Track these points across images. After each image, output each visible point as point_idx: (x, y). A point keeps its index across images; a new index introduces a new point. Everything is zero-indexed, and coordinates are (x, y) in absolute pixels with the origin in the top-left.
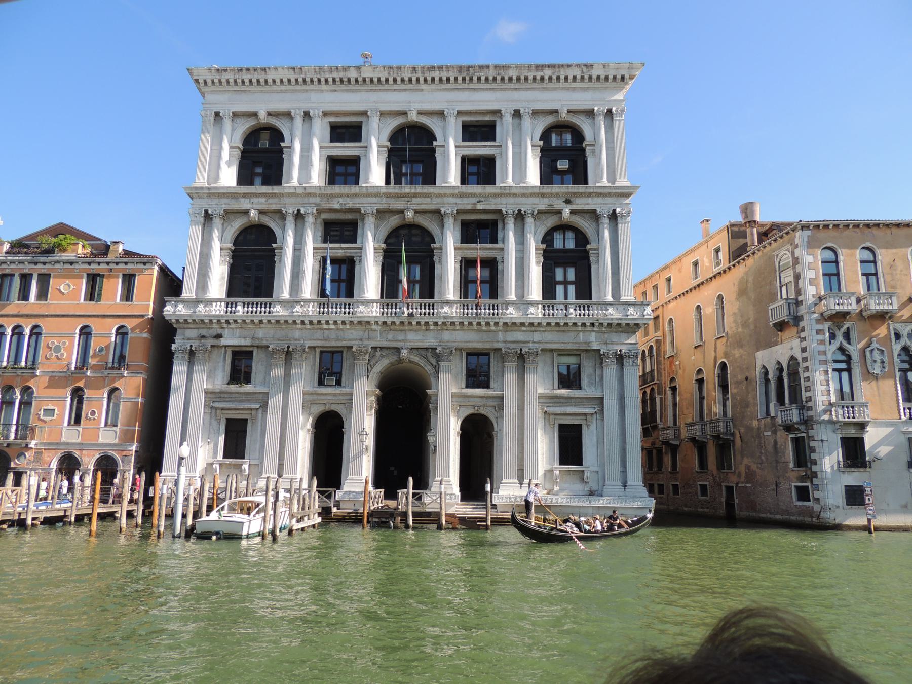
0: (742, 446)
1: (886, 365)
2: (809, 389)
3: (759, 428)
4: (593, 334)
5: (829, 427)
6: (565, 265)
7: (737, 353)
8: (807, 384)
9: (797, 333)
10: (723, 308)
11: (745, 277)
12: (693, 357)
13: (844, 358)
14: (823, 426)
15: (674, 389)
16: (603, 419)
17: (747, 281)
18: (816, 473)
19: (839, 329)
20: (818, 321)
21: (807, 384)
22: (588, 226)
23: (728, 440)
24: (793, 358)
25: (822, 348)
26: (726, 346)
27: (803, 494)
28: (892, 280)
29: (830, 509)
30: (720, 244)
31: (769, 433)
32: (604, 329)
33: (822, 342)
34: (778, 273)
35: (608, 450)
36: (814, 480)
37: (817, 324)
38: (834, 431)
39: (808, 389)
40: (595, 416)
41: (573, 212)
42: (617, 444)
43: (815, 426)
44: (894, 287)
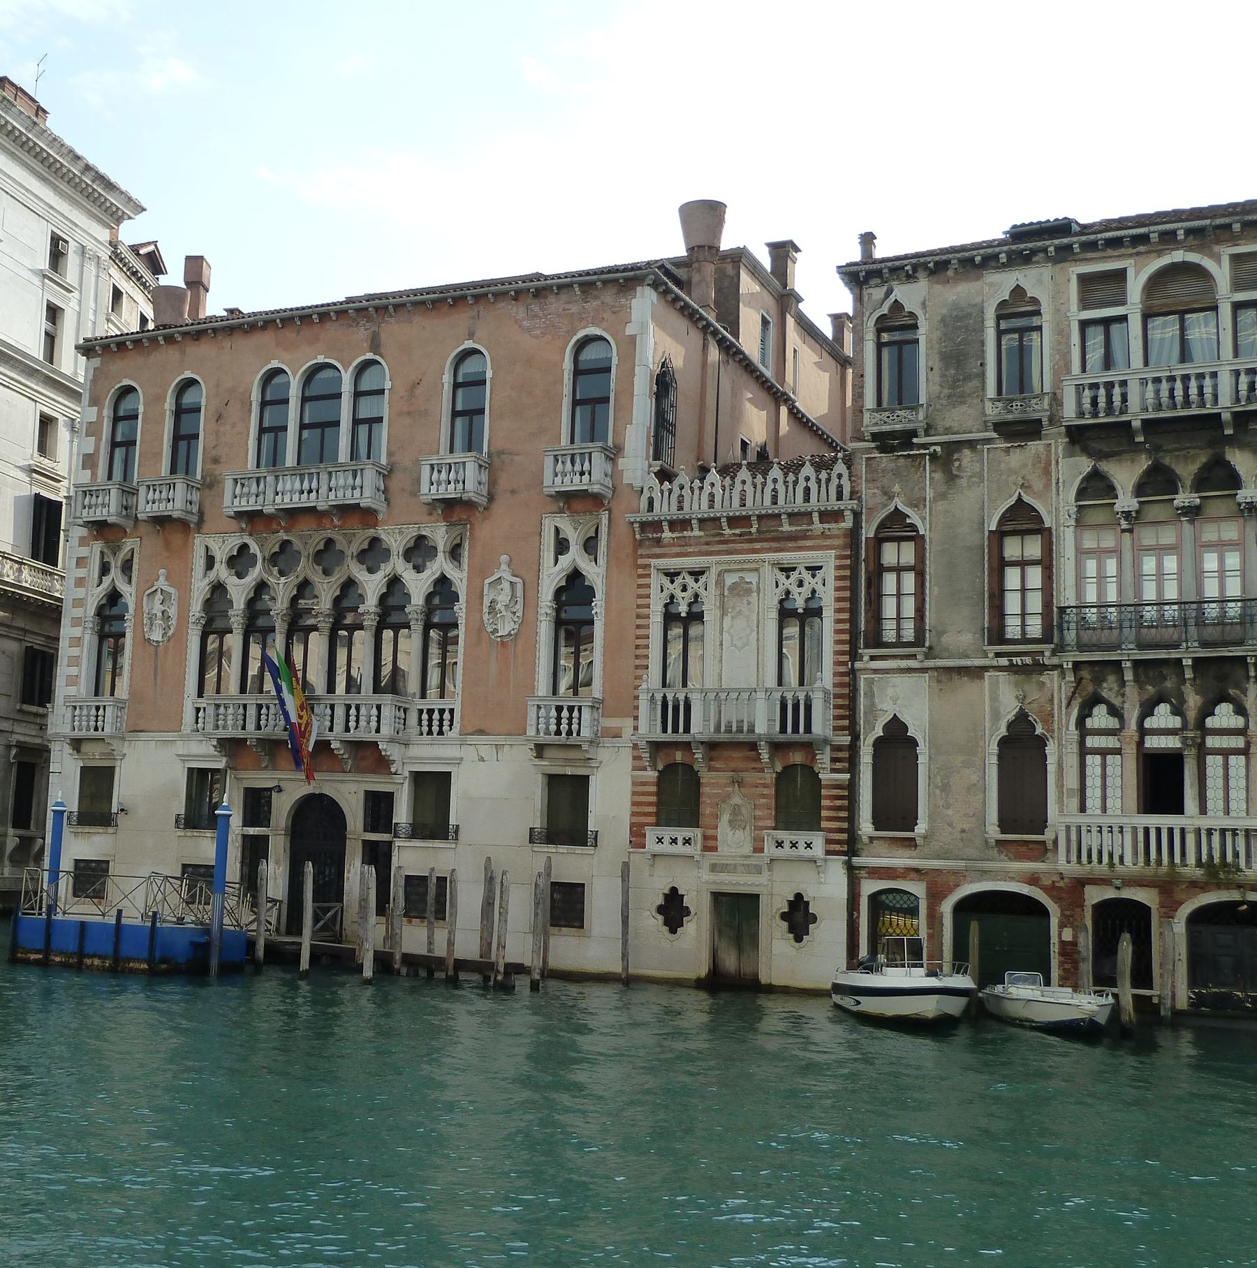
1: (173, 622)
20: (83, 542)
25: (80, 593)
33: (80, 582)
44: (216, 461)
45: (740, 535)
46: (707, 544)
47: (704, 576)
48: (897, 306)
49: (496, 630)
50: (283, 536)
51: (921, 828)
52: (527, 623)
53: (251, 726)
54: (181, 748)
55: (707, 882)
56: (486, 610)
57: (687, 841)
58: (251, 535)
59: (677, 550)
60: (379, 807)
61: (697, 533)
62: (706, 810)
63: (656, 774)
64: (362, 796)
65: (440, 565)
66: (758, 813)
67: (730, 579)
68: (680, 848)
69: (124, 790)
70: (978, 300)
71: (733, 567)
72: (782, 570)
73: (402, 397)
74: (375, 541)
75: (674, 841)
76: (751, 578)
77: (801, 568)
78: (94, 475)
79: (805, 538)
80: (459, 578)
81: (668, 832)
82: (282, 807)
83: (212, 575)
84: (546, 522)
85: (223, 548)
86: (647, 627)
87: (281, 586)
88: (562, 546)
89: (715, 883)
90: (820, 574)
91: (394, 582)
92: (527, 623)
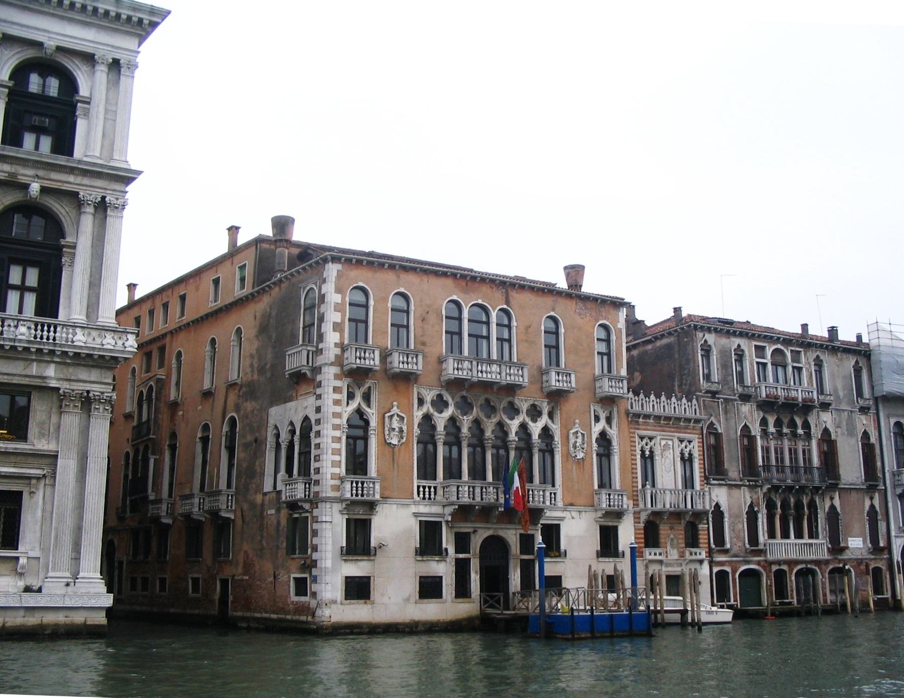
0: (243, 528)
1: (405, 434)
2: (318, 458)
3: (263, 505)
4: (52, 367)
5: (337, 507)
6: (25, 264)
7: (249, 406)
9: (314, 388)
10: (241, 344)
11: (268, 310)
12: (200, 407)
13: (362, 423)
14: (328, 505)
15: (173, 448)
16: (54, 485)
17: (270, 315)
18: (316, 561)
19: (359, 388)
20: (337, 377)
21: (318, 452)
22: (64, 213)
23: (228, 519)
24: (306, 419)
25: (338, 409)
26: (239, 396)
27: (302, 587)
28: (422, 336)
29: (326, 604)
30: (247, 262)
31: (273, 511)
32: (68, 361)
33: (337, 402)
35: (57, 529)
36: (313, 570)
37: (335, 379)
38: (340, 511)
39: (317, 459)
40: (42, 482)
41: (44, 190)
42: (69, 522)
43: (320, 505)
44: (424, 344)
45: (667, 424)
46: (655, 426)
47: (655, 439)
48: (706, 341)
49: (576, 456)
50: (464, 393)
51: (728, 546)
52: (588, 454)
53: (478, 499)
54: (414, 509)
55: (666, 571)
56: (571, 445)
57: (660, 554)
58: (447, 390)
59: (644, 427)
60: (527, 542)
61: (651, 421)
62: (662, 541)
63: (644, 525)
64: (518, 536)
65: (544, 420)
66: (680, 541)
67: (663, 442)
68: (658, 557)
69: (376, 535)
70: (729, 346)
71: (664, 437)
72: (680, 441)
73: (522, 332)
74: (511, 404)
75: (655, 554)
76: (670, 443)
77: (686, 441)
78: (342, 336)
79: (687, 429)
80: (556, 429)
81: (653, 550)
82: (476, 542)
83: (424, 409)
84: (592, 407)
85: (429, 396)
86: (636, 460)
87: (466, 421)
88: (597, 419)
89: (668, 571)
90: (692, 444)
91: (523, 427)
92: (588, 454)
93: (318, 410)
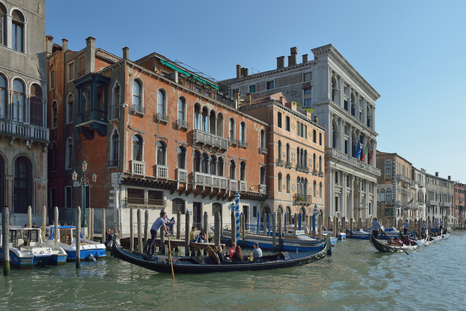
8: (394, 196)
18: (394, 217)
21: (394, 196)
34: (385, 165)
93: (394, 187)
